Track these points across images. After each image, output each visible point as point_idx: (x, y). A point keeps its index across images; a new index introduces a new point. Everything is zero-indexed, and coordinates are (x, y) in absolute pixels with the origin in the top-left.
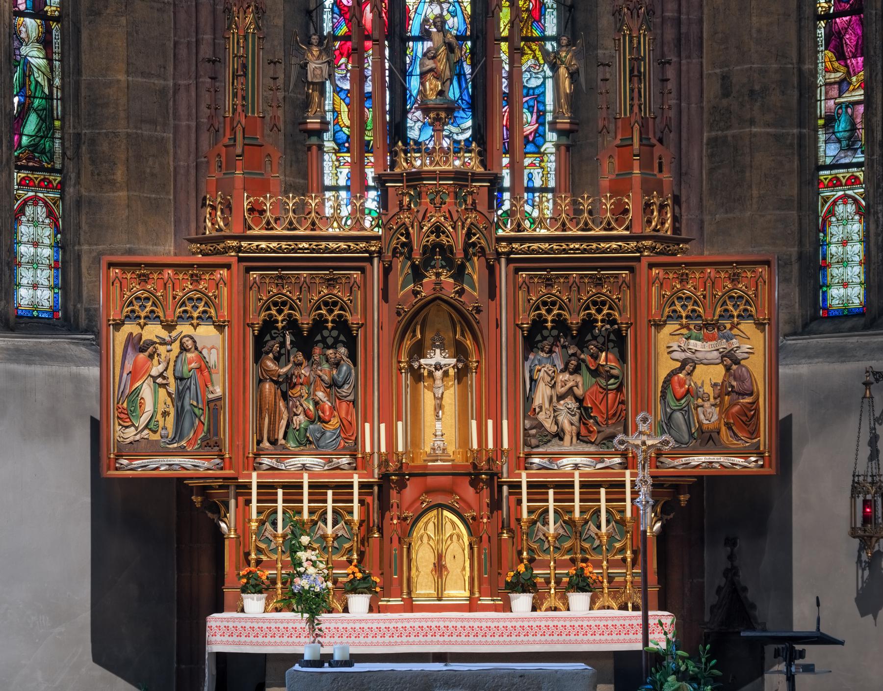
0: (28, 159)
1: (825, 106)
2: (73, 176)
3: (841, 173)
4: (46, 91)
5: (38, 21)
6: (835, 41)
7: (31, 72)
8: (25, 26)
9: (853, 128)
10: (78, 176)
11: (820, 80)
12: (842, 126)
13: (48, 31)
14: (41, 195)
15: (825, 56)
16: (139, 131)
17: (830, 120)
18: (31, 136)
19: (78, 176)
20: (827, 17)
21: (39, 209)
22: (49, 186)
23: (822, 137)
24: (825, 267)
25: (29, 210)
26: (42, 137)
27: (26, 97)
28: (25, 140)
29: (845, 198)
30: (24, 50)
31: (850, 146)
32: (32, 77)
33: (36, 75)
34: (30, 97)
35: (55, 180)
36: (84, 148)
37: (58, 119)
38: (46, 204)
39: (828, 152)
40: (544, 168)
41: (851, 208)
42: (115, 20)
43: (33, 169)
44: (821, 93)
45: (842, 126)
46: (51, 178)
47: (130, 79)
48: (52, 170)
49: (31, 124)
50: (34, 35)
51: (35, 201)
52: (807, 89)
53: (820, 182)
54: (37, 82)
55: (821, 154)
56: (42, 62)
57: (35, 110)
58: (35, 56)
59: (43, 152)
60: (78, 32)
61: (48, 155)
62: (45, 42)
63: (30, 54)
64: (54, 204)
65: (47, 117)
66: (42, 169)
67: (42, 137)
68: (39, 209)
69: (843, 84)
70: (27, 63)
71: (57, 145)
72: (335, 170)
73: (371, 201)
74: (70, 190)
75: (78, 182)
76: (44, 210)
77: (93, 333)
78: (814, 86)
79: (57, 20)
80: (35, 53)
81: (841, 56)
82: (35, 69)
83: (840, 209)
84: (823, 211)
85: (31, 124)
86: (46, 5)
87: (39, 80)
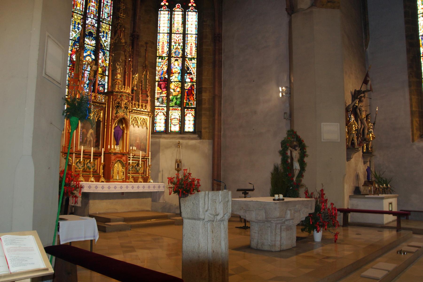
1: (156, 96)
3: (160, 108)
6: (159, 86)
9: (163, 100)
11: (156, 92)
12: (160, 100)
15: (157, 88)
17: (158, 99)
20: (158, 81)
23: (156, 101)
24: (156, 123)
29: (161, 112)
31: (162, 103)
39: (157, 104)
41: (162, 114)
44: (156, 94)
45: (160, 100)
53: (155, 109)
55: (156, 104)
69: (161, 93)
78: (155, 93)
81: (161, 88)
83: (159, 114)
84: (156, 114)
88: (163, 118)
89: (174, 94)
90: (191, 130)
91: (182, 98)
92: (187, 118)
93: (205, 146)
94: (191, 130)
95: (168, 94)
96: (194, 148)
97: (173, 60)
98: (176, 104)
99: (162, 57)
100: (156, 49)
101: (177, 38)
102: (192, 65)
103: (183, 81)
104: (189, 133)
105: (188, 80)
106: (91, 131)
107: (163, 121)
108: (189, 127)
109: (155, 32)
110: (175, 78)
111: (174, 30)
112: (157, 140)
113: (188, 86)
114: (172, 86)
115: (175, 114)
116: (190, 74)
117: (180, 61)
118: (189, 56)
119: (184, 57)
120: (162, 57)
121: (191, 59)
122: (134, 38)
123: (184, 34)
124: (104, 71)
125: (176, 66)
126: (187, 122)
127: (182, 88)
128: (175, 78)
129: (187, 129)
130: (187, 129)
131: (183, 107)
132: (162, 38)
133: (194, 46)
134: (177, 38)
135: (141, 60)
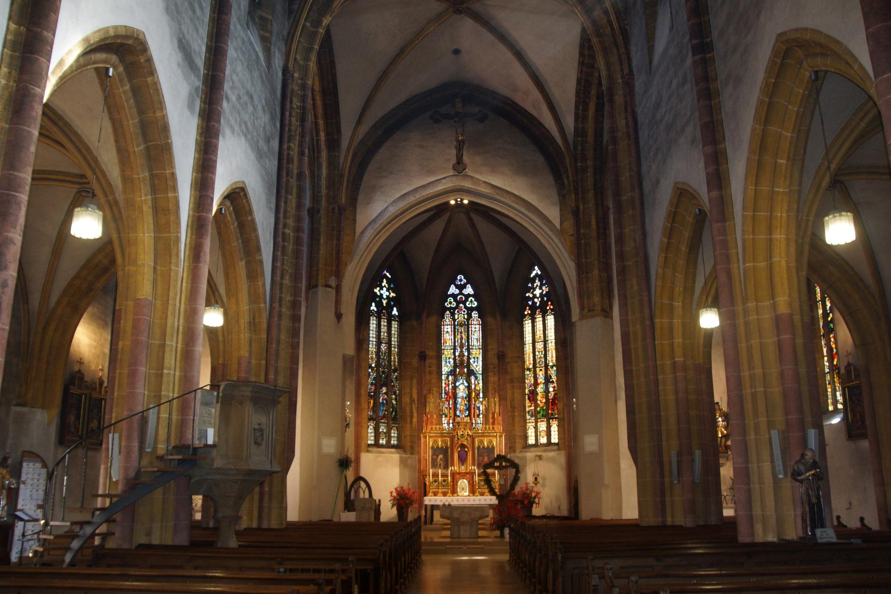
1: (527, 409)
6: (529, 399)
15: (527, 401)
39: (528, 417)
40: (480, 420)
52: (525, 407)
58: (394, 402)
62: (396, 399)
65: (396, 412)
72: (444, 420)
73: (451, 425)
88: (533, 430)
89: (541, 405)
90: (556, 441)
91: (547, 409)
92: (552, 429)
93: (561, 457)
94: (556, 441)
95: (536, 406)
96: (552, 460)
97: (538, 369)
98: (543, 416)
99: (529, 369)
100: (524, 362)
101: (540, 346)
102: (553, 372)
103: (547, 391)
104: (554, 444)
105: (551, 389)
106: (441, 456)
107: (533, 434)
108: (555, 439)
109: (522, 343)
110: (540, 389)
111: (537, 337)
112: (524, 454)
113: (551, 396)
114: (539, 398)
115: (542, 426)
116: (553, 382)
117: (543, 369)
118: (551, 364)
119: (546, 366)
120: (529, 369)
121: (552, 367)
122: (501, 357)
123: (545, 341)
124: (479, 394)
125: (541, 375)
126: (552, 433)
127: (547, 397)
128: (540, 389)
129: (553, 441)
130: (553, 441)
131: (549, 418)
132: (528, 348)
133: (554, 352)
134: (540, 346)
135: (508, 377)
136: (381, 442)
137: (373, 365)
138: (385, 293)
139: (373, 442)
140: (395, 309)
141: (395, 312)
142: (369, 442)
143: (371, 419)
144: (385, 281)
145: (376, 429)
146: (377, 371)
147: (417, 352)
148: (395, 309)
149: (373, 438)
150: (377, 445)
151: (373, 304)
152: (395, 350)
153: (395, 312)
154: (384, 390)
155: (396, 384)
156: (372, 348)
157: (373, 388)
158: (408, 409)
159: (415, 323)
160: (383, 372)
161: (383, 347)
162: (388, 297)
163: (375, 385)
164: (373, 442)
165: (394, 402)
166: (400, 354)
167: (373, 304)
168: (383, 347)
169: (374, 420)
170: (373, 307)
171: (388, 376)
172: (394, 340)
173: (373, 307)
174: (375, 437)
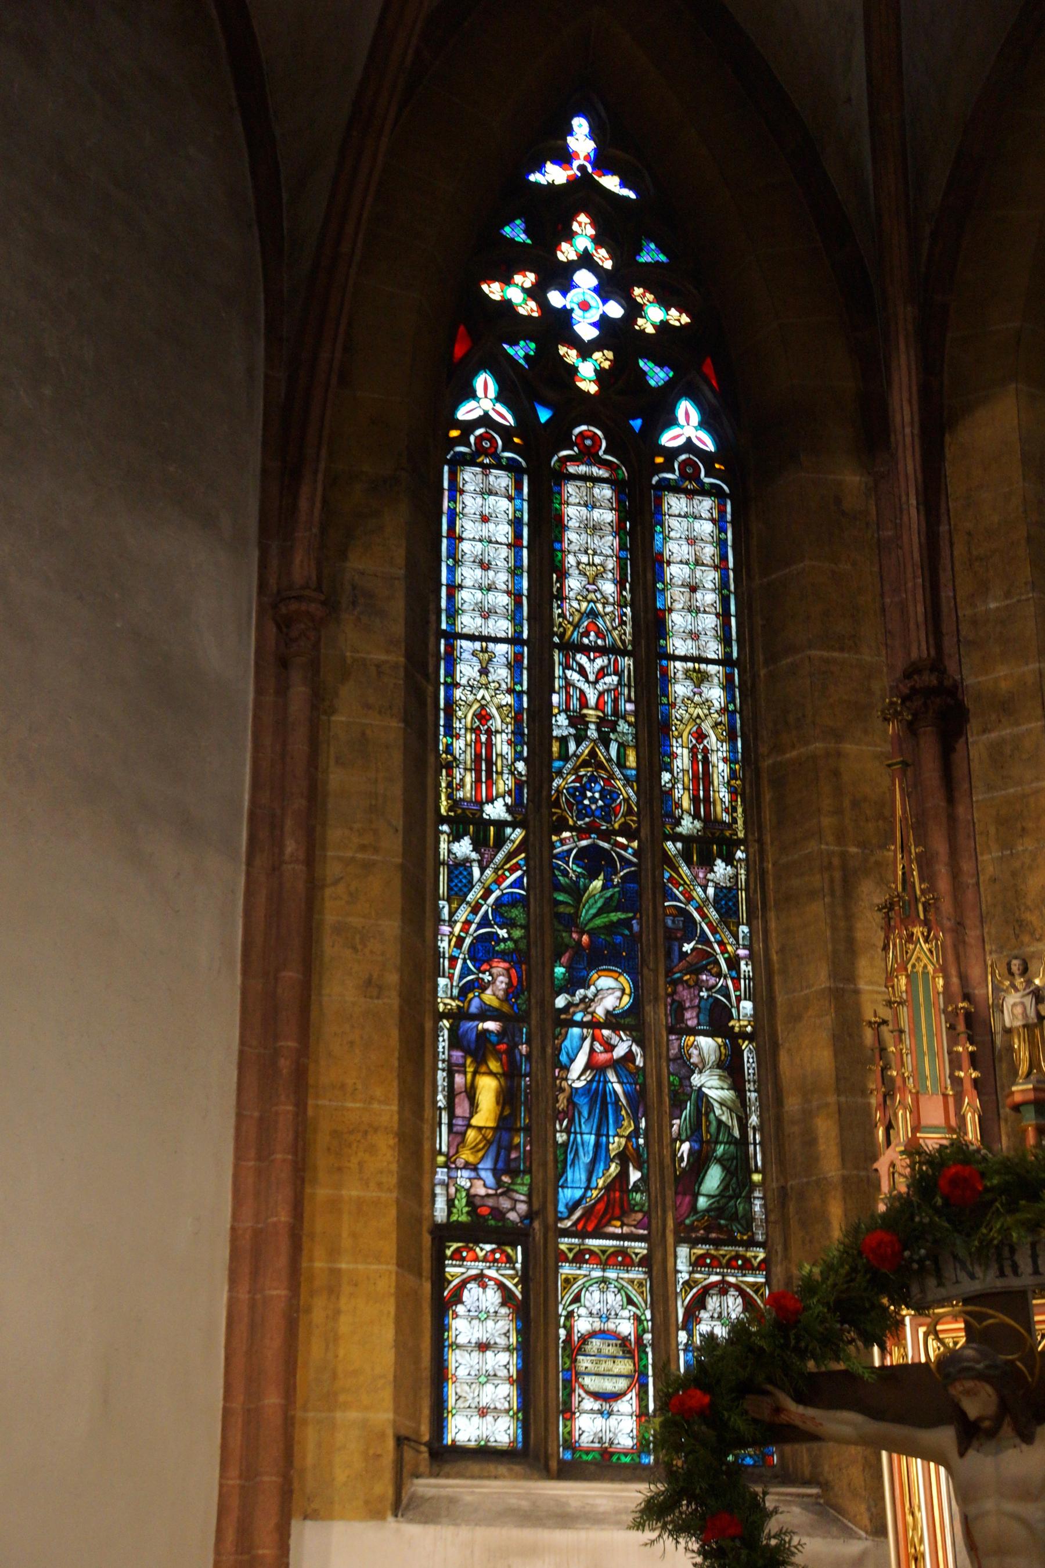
0: (708, 1229)
2: (779, 1248)
4: (736, 1133)
5: (719, 1040)
7: (710, 1108)
8: (697, 1047)
10: (786, 1248)
13: (736, 1054)
14: (732, 1280)
16: (863, 1173)
18: (713, 1197)
19: (786, 1248)
21: (731, 1300)
22: (748, 1266)
25: (712, 1302)
26: (731, 1198)
27: (701, 1142)
28: (702, 1202)
30: (696, 1080)
32: (712, 1115)
33: (718, 1112)
34: (708, 1142)
35: (756, 1257)
36: (792, 1208)
37: (757, 1171)
38: (742, 1293)
42: (818, 1021)
43: (717, 1243)
46: (749, 1254)
47: (843, 1099)
48: (752, 1243)
49: (713, 1179)
50: (713, 1058)
51: (723, 1288)
54: (720, 1122)
56: (728, 1094)
57: (720, 1161)
58: (711, 1085)
59: (734, 1217)
60: (775, 1046)
61: (743, 1222)
62: (730, 1067)
63: (708, 1084)
64: (756, 1292)
65: (737, 1170)
66: (733, 1242)
67: (731, 1198)
68: (731, 1300)
70: (701, 1095)
71: (757, 1209)
74: (778, 1270)
75: (786, 1257)
76: (739, 1300)
77: (819, 1484)
79: (750, 1037)
80: (715, 1082)
82: (716, 1105)
85: (713, 1179)
86: (731, 1018)
87: (724, 1118)
136: (588, 1426)
137: (496, 811)
138: (585, 304)
139: (502, 1431)
140: (686, 410)
141: (687, 427)
142: (463, 1429)
143: (480, 1227)
144: (583, 227)
145: (534, 1312)
146: (537, 853)
147: (882, 685)
148: (686, 410)
149: (502, 1394)
150: (540, 1449)
151: (485, 383)
152: (700, 699)
153: (687, 427)
154: (610, 992)
155: (737, 943)
156: (481, 680)
157: (498, 981)
158: (826, 1128)
159: (852, 480)
160: (594, 861)
161: (589, 681)
162: (615, 335)
163: (516, 958)
164: (502, 1431)
165: (711, 1085)
166: (754, 720)
167: (485, 383)
168: (589, 681)
169: (505, 1235)
170: (484, 401)
171: (642, 887)
172: (695, 624)
173: (484, 401)
174: (525, 1381)
